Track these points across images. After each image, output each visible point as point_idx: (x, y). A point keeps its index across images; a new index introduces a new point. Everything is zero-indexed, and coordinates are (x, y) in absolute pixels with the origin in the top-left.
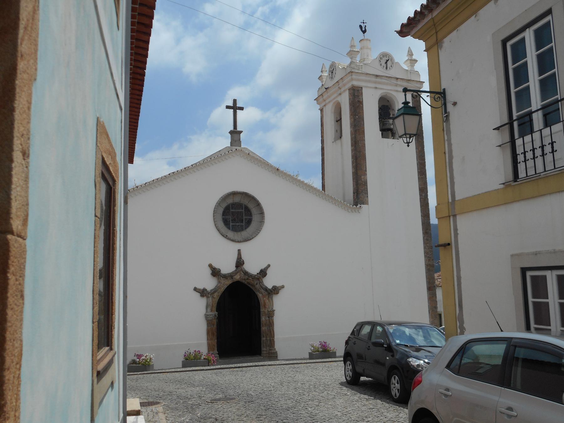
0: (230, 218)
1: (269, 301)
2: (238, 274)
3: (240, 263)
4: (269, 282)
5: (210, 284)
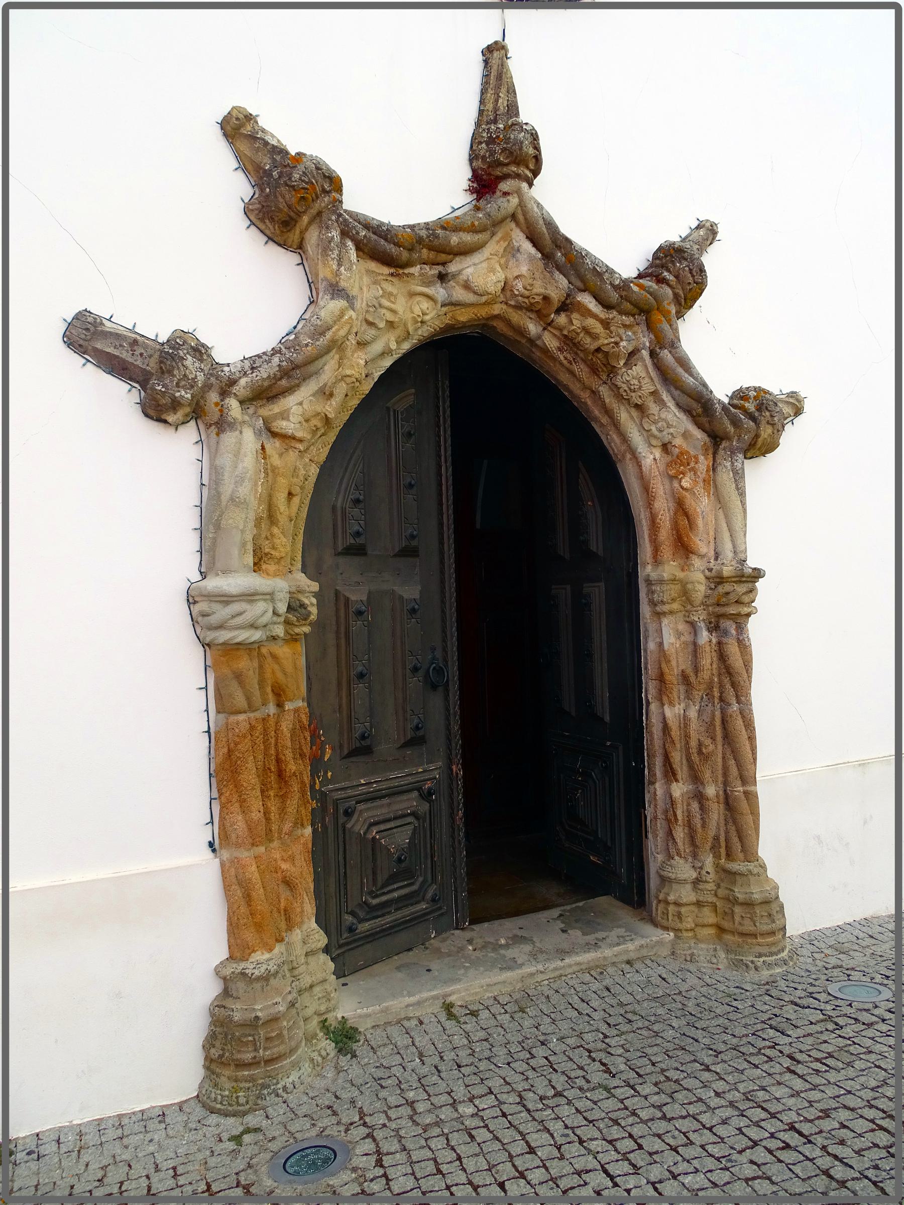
1: (720, 500)
2: (494, 247)
3: (502, 156)
4: (720, 348)
5: (242, 302)
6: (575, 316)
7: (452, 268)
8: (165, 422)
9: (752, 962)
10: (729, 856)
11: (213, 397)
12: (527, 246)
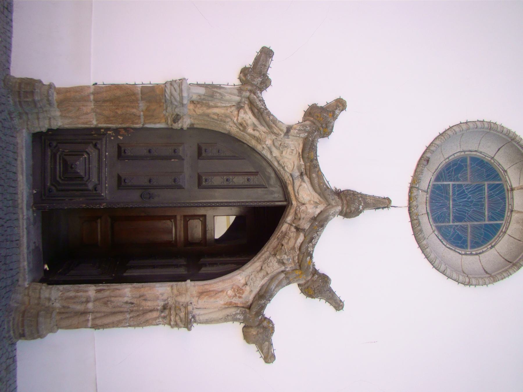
0: (468, 181)
2: (316, 197)
6: (295, 234)
7: (305, 178)
8: (241, 73)
9: (11, 315)
10: (60, 313)
11: (249, 88)
12: (318, 211)
